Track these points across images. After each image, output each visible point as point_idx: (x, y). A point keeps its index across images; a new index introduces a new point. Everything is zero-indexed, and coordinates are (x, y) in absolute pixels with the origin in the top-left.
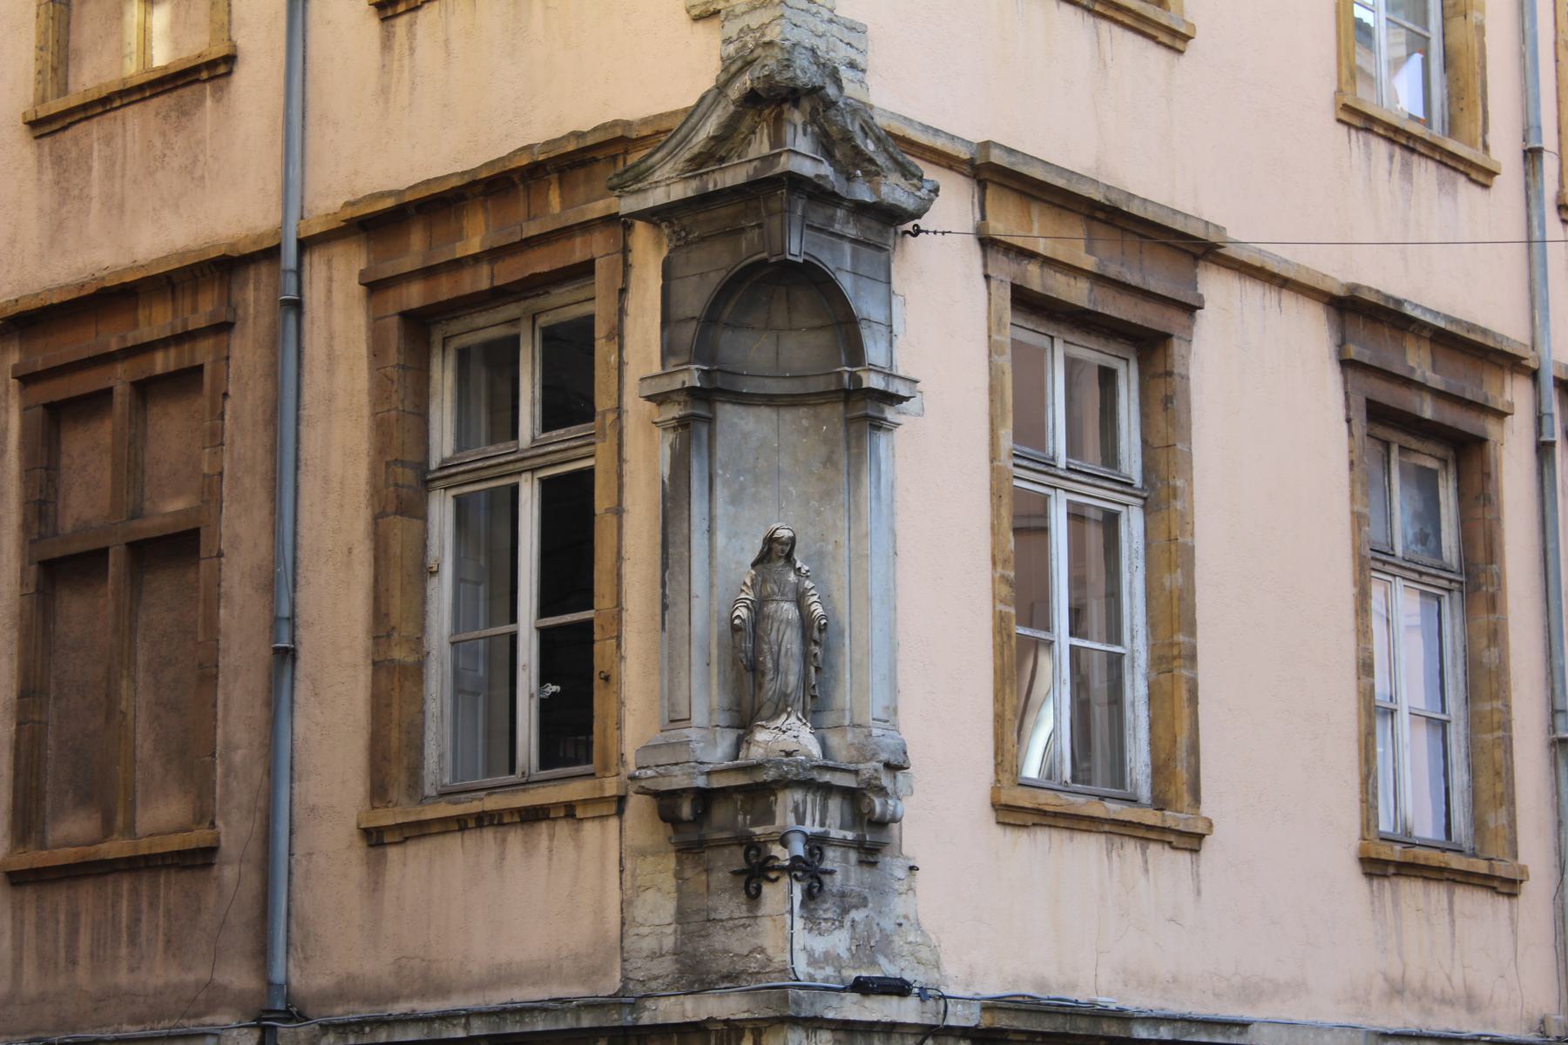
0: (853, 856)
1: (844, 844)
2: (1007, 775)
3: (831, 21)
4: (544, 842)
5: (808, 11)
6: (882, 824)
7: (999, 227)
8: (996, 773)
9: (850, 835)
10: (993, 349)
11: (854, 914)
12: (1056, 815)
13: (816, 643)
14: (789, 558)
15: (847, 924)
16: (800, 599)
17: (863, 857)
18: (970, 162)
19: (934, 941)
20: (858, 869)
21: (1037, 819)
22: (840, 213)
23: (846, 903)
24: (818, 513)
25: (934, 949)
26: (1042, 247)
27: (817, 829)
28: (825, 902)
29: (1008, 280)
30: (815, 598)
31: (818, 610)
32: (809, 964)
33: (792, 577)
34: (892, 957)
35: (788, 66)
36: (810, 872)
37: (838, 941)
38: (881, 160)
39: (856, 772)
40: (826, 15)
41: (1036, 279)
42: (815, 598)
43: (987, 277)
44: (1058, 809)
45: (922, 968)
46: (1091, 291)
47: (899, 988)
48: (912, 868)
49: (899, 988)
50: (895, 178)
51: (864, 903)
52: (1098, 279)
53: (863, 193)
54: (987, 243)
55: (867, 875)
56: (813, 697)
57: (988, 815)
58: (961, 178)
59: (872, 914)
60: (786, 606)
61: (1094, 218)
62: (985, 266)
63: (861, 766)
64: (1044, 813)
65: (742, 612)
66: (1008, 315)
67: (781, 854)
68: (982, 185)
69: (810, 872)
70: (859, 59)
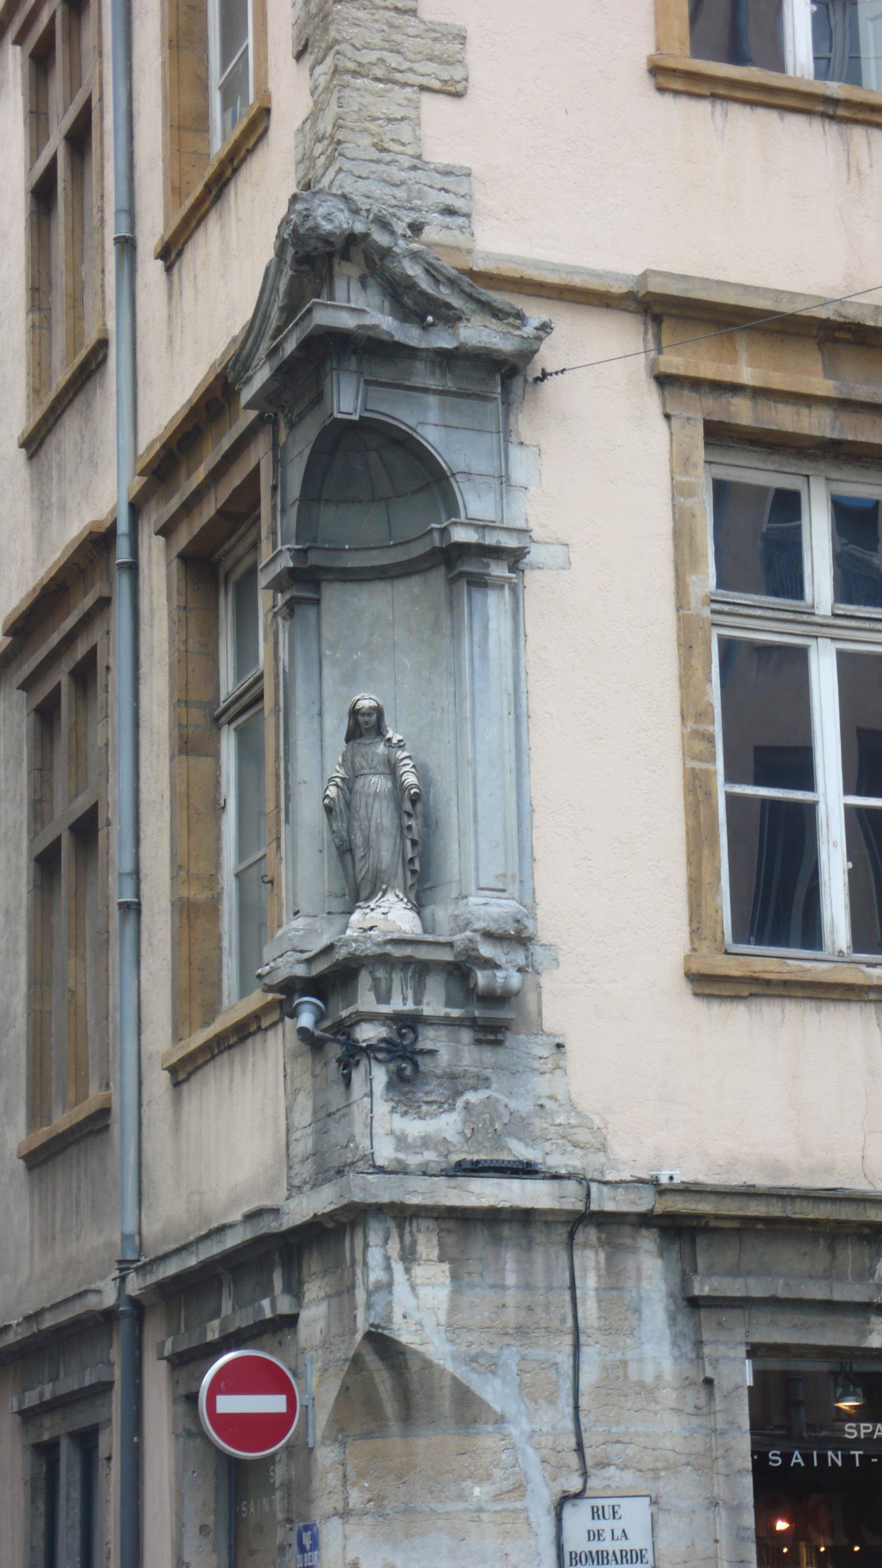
0: (466, 1036)
1: (447, 1022)
2: (707, 943)
3: (414, 168)
4: (251, 1060)
5: (378, 162)
6: (499, 998)
7: (675, 362)
8: (692, 942)
9: (455, 1013)
10: (679, 491)
11: (472, 1097)
12: (786, 983)
13: (410, 815)
14: (379, 730)
15: (460, 1103)
16: (392, 769)
17: (481, 1036)
18: (631, 296)
19: (597, 1121)
20: (475, 1049)
21: (755, 989)
22: (419, 366)
23: (456, 1083)
24: (429, 681)
25: (595, 1131)
26: (747, 375)
27: (410, 1006)
28: (427, 1084)
29: (700, 417)
30: (407, 768)
31: (410, 779)
32: (397, 1150)
33: (381, 748)
34: (532, 1141)
35: (307, 216)
36: (403, 1053)
37: (447, 1125)
38: (457, 302)
39: (451, 945)
40: (406, 162)
41: (743, 413)
42: (407, 768)
43: (667, 417)
44: (787, 977)
45: (578, 1151)
46: (835, 419)
47: (524, 1170)
48: (559, 1046)
49: (524, 1170)
50: (477, 320)
51: (484, 1082)
52: (843, 404)
53: (443, 340)
54: (664, 381)
55: (488, 1055)
56: (414, 872)
57: (685, 989)
58: (628, 316)
59: (495, 1095)
60: (374, 779)
61: (837, 340)
62: (664, 405)
63: (455, 938)
64: (768, 983)
65: (332, 791)
66: (699, 453)
67: (368, 1033)
68: (657, 320)
69: (403, 1053)
70: (458, 203)
